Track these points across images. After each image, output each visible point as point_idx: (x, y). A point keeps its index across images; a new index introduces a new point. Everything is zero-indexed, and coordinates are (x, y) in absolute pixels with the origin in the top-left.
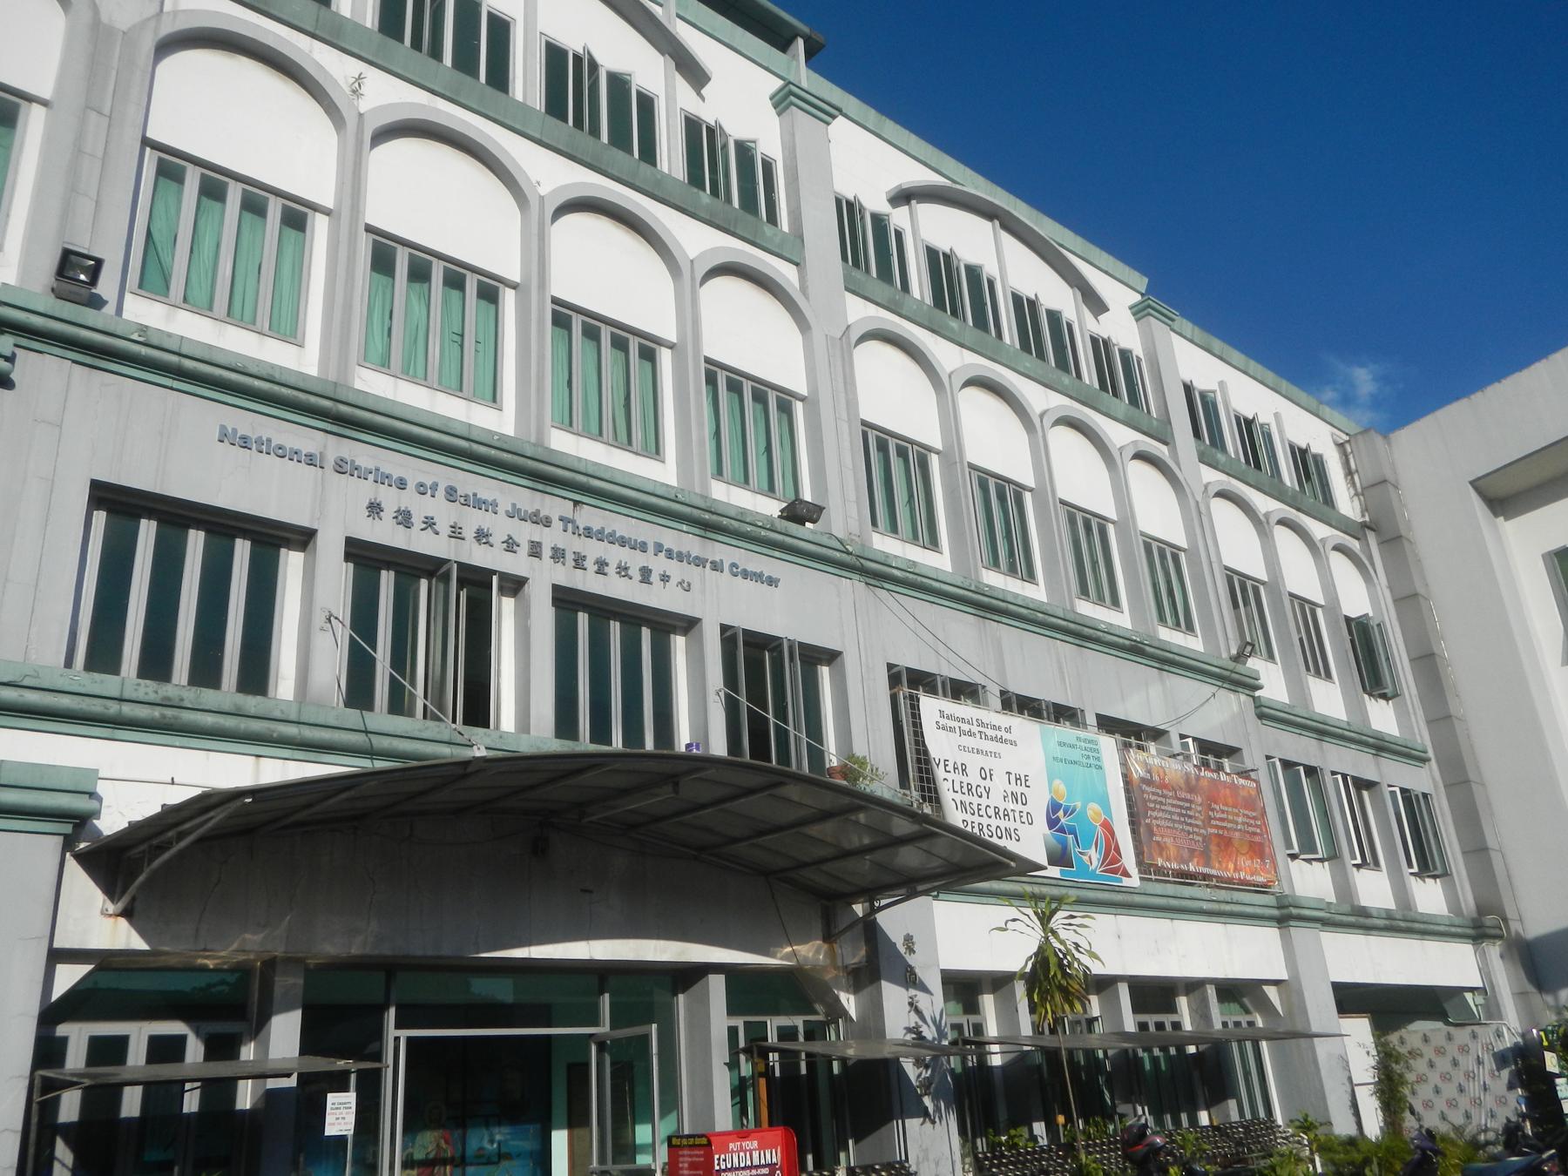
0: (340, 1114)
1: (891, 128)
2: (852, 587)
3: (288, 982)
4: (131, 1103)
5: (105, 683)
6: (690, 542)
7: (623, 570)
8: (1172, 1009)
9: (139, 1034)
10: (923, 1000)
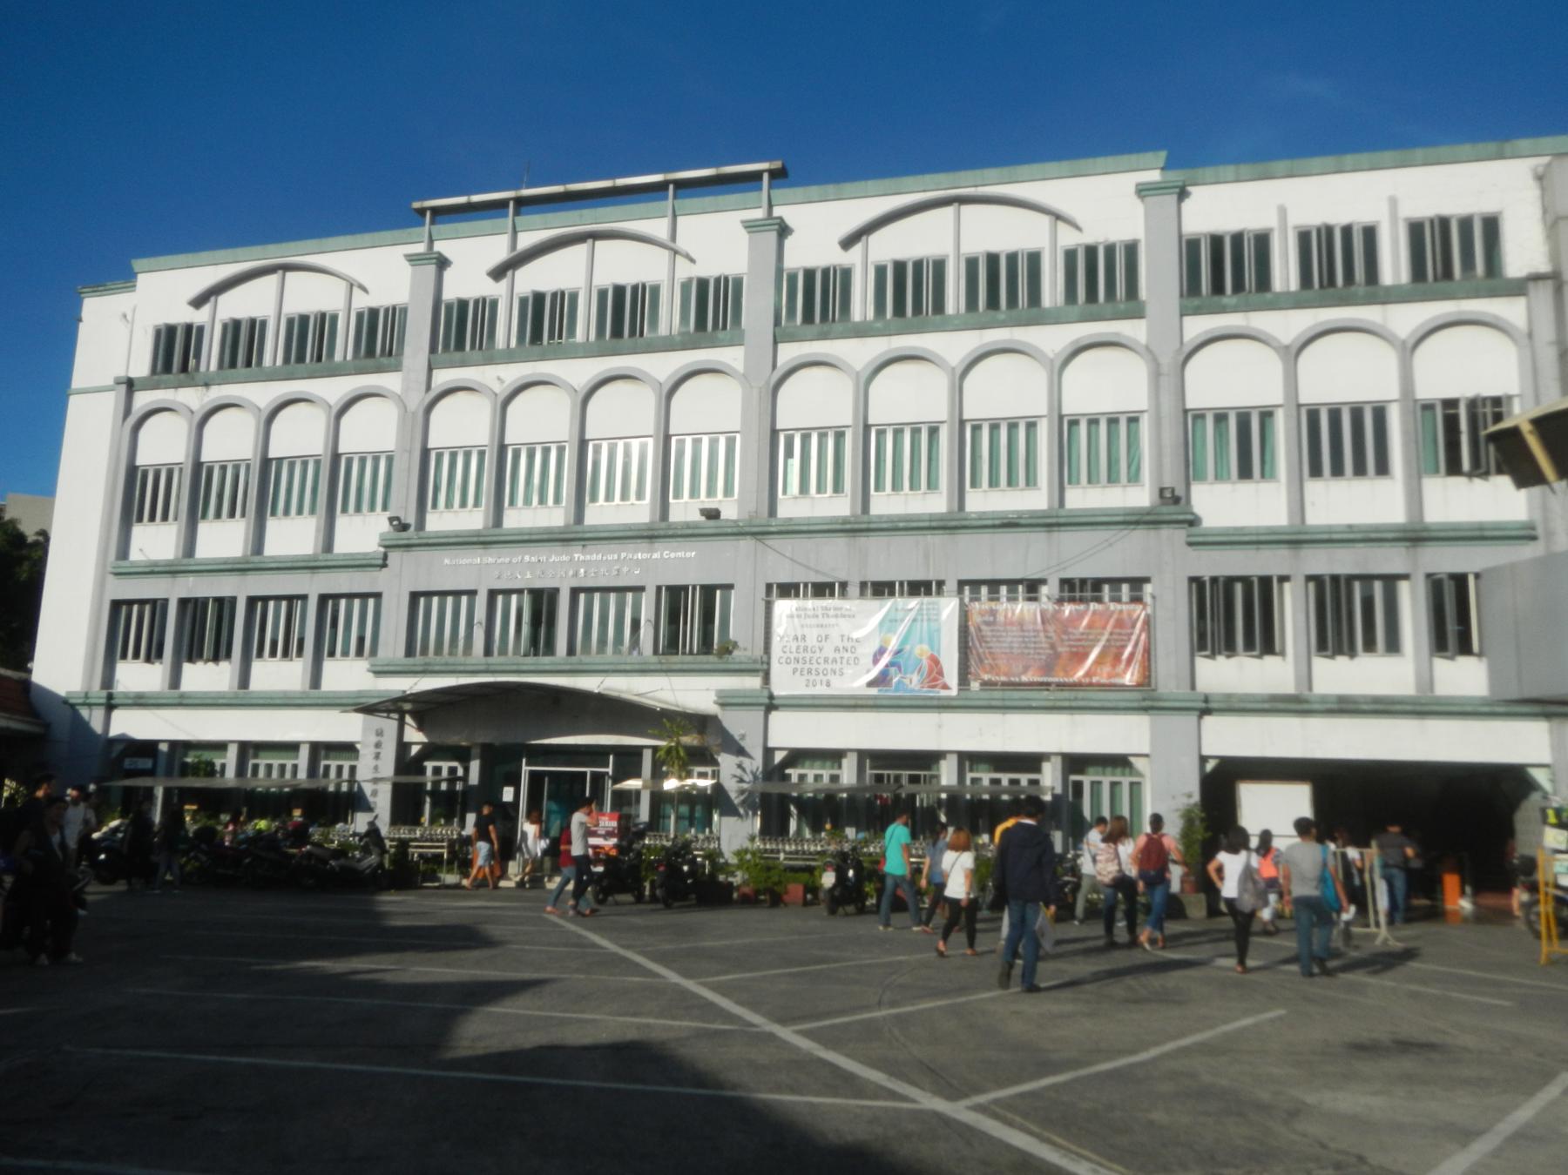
0: (508, 794)
1: (848, 187)
2: (746, 544)
3: (476, 751)
4: (444, 786)
5: (411, 660)
6: (644, 544)
8: (1038, 770)
9: (445, 766)
10: (746, 762)
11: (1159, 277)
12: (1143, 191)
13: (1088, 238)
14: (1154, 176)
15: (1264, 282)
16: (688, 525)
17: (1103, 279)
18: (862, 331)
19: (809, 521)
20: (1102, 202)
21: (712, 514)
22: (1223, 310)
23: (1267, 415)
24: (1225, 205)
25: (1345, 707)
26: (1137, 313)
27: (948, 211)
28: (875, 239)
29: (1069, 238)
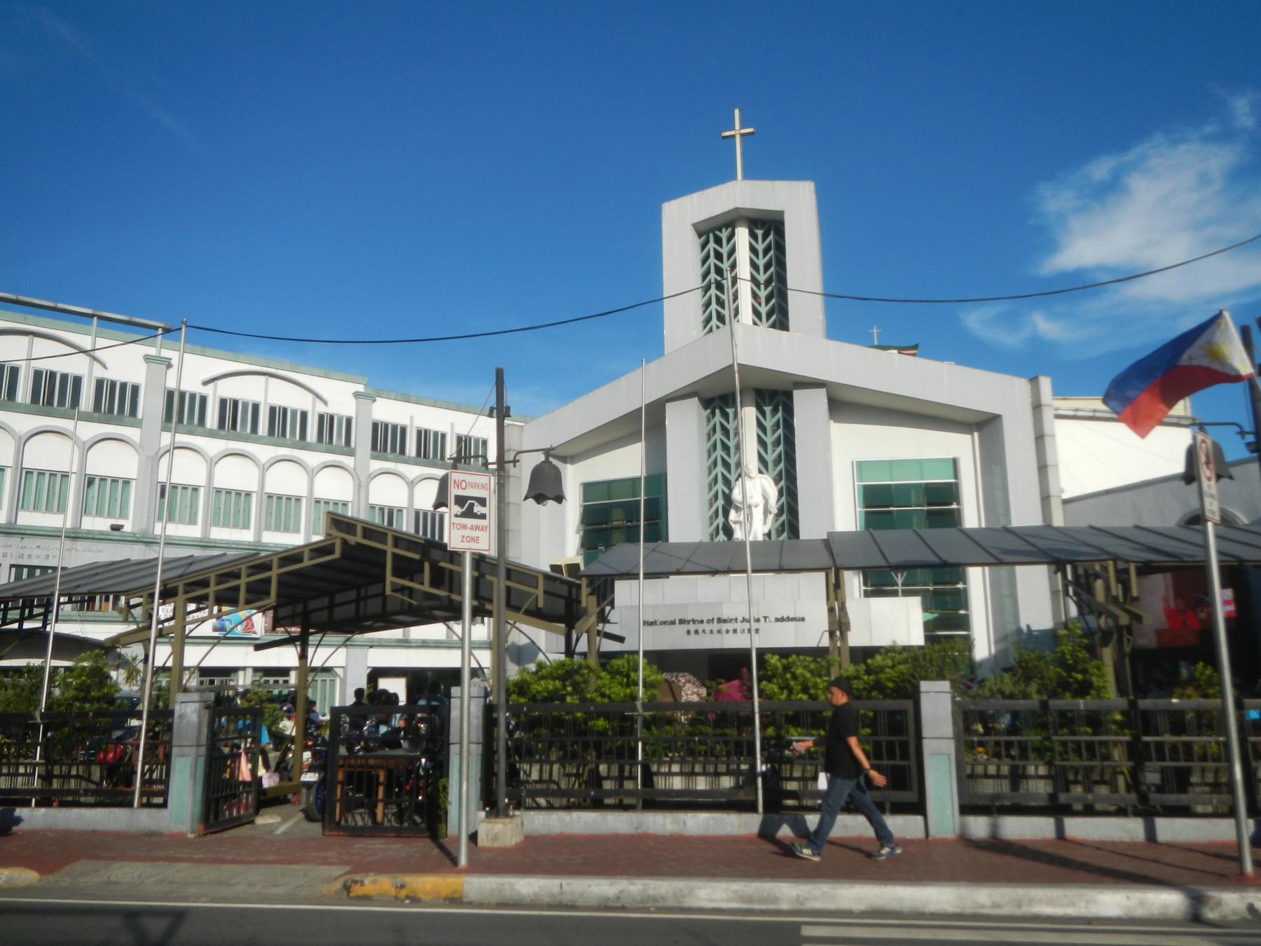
1: (208, 350)
6: (68, 543)
7: (38, 557)
11: (362, 438)
12: (357, 395)
13: (329, 410)
14: (361, 388)
15: (403, 451)
16: (102, 533)
17: (332, 432)
18: (211, 434)
19: (181, 539)
20: (339, 396)
21: (116, 528)
22: (387, 460)
23: (400, 510)
24: (389, 411)
25: (424, 644)
26: (351, 453)
27: (263, 378)
28: (220, 382)
29: (321, 408)
